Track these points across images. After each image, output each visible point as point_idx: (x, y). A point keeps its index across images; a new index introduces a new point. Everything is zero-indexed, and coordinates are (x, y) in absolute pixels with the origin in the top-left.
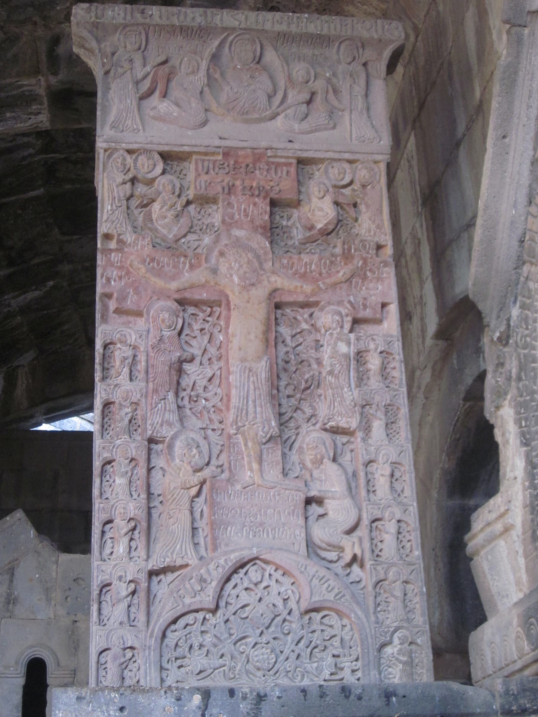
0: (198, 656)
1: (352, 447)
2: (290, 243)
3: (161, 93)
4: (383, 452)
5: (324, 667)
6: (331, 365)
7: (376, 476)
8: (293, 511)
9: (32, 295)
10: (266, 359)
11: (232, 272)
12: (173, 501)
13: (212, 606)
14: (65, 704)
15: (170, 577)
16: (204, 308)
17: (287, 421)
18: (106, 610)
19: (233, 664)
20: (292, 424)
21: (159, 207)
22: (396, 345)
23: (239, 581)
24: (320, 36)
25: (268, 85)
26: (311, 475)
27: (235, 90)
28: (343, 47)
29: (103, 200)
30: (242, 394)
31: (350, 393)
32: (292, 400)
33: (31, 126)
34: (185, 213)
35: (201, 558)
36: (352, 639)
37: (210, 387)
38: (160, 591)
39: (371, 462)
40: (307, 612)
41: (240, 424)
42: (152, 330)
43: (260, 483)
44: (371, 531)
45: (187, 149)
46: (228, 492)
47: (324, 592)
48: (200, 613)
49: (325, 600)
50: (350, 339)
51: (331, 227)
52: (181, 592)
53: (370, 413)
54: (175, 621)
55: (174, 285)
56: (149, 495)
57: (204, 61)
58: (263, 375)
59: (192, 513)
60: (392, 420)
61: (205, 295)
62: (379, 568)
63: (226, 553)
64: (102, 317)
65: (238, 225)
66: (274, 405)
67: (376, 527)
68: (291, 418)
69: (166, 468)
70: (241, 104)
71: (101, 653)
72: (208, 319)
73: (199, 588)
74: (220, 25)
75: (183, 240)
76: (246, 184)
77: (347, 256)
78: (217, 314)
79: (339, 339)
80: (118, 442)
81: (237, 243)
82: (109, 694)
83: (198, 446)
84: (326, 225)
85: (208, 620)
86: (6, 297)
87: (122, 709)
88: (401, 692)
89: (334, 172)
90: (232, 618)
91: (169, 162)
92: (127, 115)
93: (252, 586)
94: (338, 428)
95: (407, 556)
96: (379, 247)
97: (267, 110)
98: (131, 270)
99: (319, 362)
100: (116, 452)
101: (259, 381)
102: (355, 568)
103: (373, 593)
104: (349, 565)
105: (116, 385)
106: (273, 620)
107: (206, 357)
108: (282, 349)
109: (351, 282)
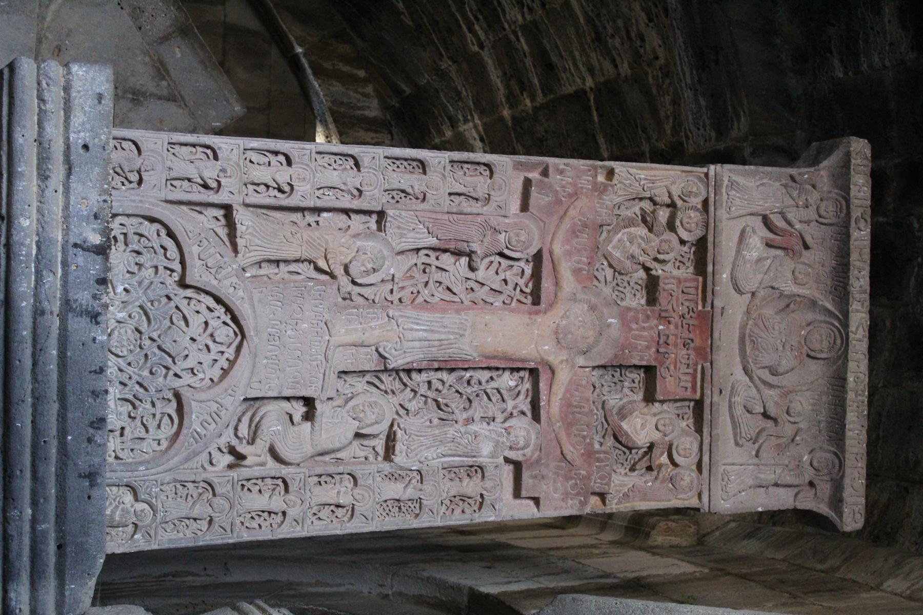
1: (371, 458)
2: (606, 389)
3: (772, 240)
4: (366, 495)
8: (297, 383)
10: (475, 355)
13: (188, 281)
15: (223, 232)
16: (530, 285)
17: (401, 379)
20: (397, 385)
21: (643, 235)
24: (843, 427)
25: (785, 364)
27: (776, 328)
28: (830, 456)
33: (690, 131)
34: (635, 266)
37: (440, 289)
38: (206, 219)
40: (177, 396)
41: (400, 321)
42: (507, 221)
44: (272, 478)
45: (710, 268)
48: (180, 266)
51: (623, 440)
52: (205, 242)
54: (171, 234)
55: (558, 249)
56: (318, 210)
57: (808, 292)
58: (456, 351)
59: (297, 261)
62: (229, 486)
64: (521, 164)
67: (278, 485)
69: (349, 232)
70: (762, 334)
72: (518, 289)
73: (209, 265)
74: (850, 309)
75: (605, 263)
76: (671, 337)
78: (524, 300)
84: (626, 434)
85: (170, 276)
86: (476, 117)
87: (86, 147)
88: (95, 493)
90: (172, 304)
91: (693, 249)
94: (394, 440)
95: (242, 523)
96: (602, 496)
99: (470, 421)
100: (368, 172)
102: (229, 459)
104: (232, 451)
106: (170, 356)
107: (476, 286)
108: (484, 375)
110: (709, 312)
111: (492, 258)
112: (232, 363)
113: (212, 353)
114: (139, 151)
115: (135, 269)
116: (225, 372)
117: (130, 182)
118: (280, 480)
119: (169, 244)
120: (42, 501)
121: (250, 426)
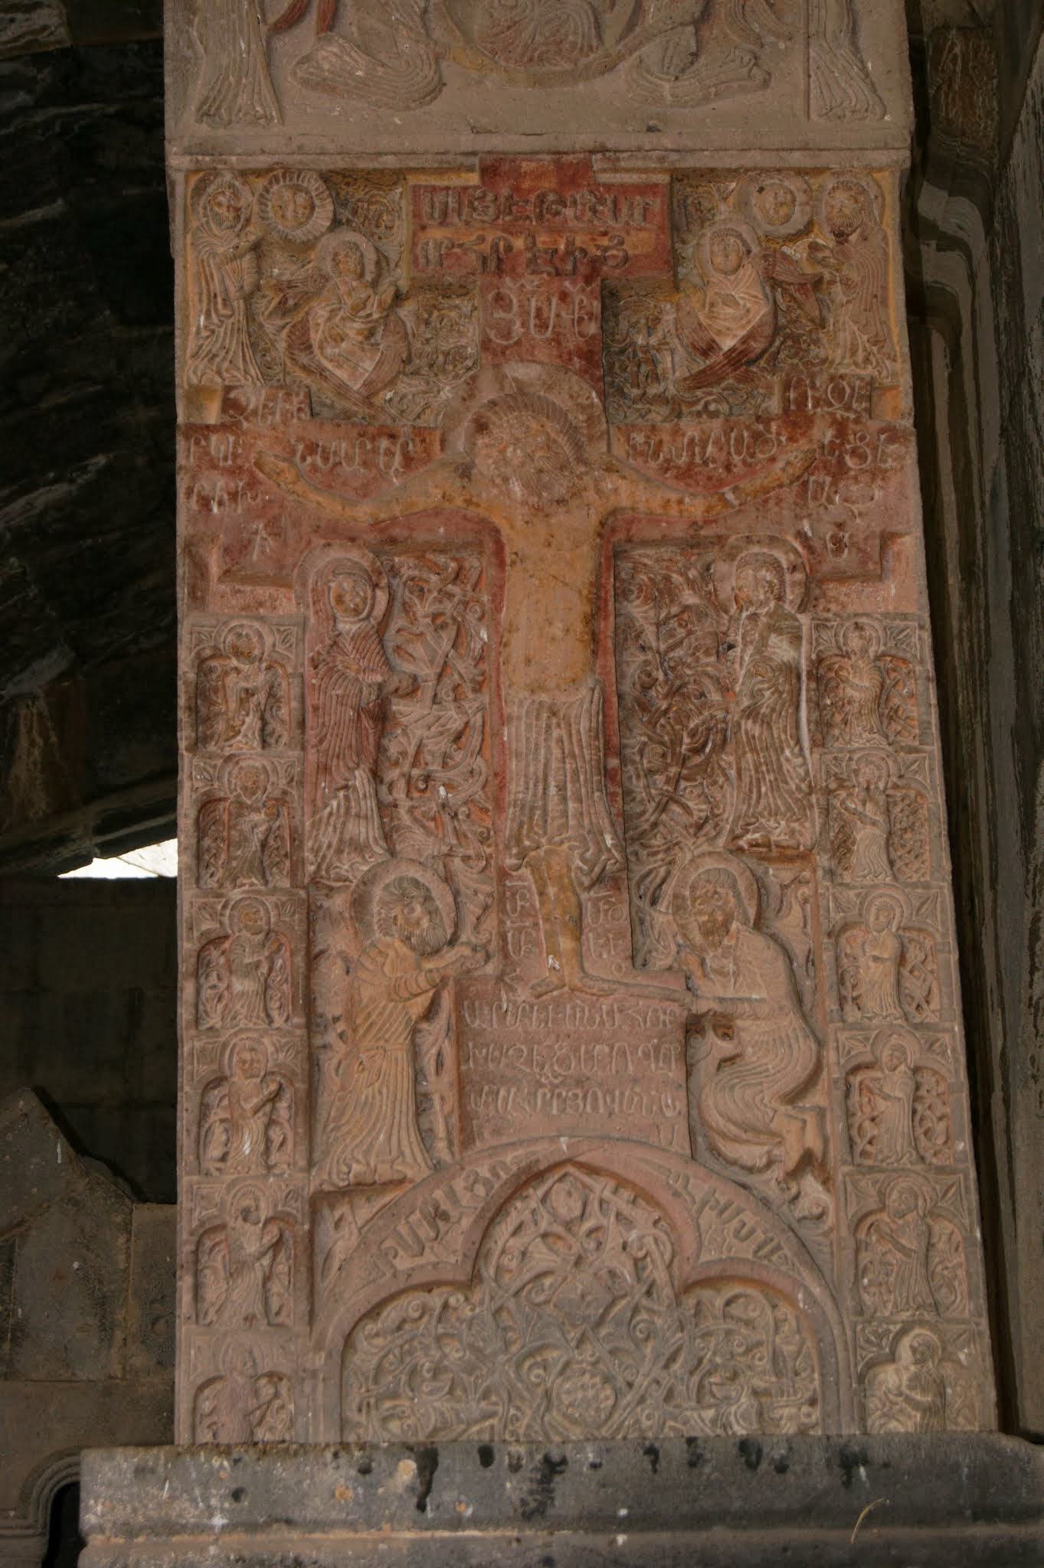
0: (431, 1393)
2: (653, 390)
3: (322, 17)
5: (732, 1418)
6: (752, 696)
7: (862, 960)
8: (657, 1049)
9: (44, 497)
11: (509, 471)
12: (368, 1030)
14: (110, 1485)
15: (365, 1211)
18: (213, 1292)
19: (512, 1411)
22: (915, 640)
23: (527, 1216)
26: (703, 963)
29: (186, 301)
30: (532, 769)
31: (800, 760)
32: (660, 779)
33: (16, 40)
35: (438, 1167)
36: (799, 1353)
37: (459, 756)
38: (340, 1243)
39: (845, 927)
42: (312, 620)
43: (577, 983)
44: (847, 1095)
45: (390, 162)
46: (500, 1007)
47: (730, 1239)
49: (732, 1259)
50: (799, 628)
51: (757, 346)
53: (846, 809)
54: (374, 1312)
58: (584, 725)
60: (904, 825)
61: (442, 530)
62: (865, 1183)
63: (494, 1150)
64: (193, 594)
65: (520, 350)
66: (612, 796)
67: (861, 1083)
68: (655, 825)
70: (526, 35)
71: (201, 1388)
77: (796, 420)
79: (772, 628)
80: (236, 894)
81: (520, 398)
82: (208, 1460)
83: (428, 898)
84: (745, 340)
88: (878, 1454)
89: (763, 204)
90: (511, 1304)
92: (238, 82)
93: (558, 1229)
97: (591, 48)
98: (260, 475)
100: (231, 917)
101: (574, 740)
103: (852, 1243)
104: (795, 1174)
105: (229, 759)
107: (448, 682)
108: (635, 660)
109: (805, 484)
110: (481, 160)
111: (390, 645)
112: (621, 1183)
113: (605, 1222)
114: (220, 1378)
115: (447, 1377)
116: (642, 1196)
117: (277, 1395)
118: (851, 1078)
119: (393, 1314)
120: (893, 1552)
121: (747, 1142)
